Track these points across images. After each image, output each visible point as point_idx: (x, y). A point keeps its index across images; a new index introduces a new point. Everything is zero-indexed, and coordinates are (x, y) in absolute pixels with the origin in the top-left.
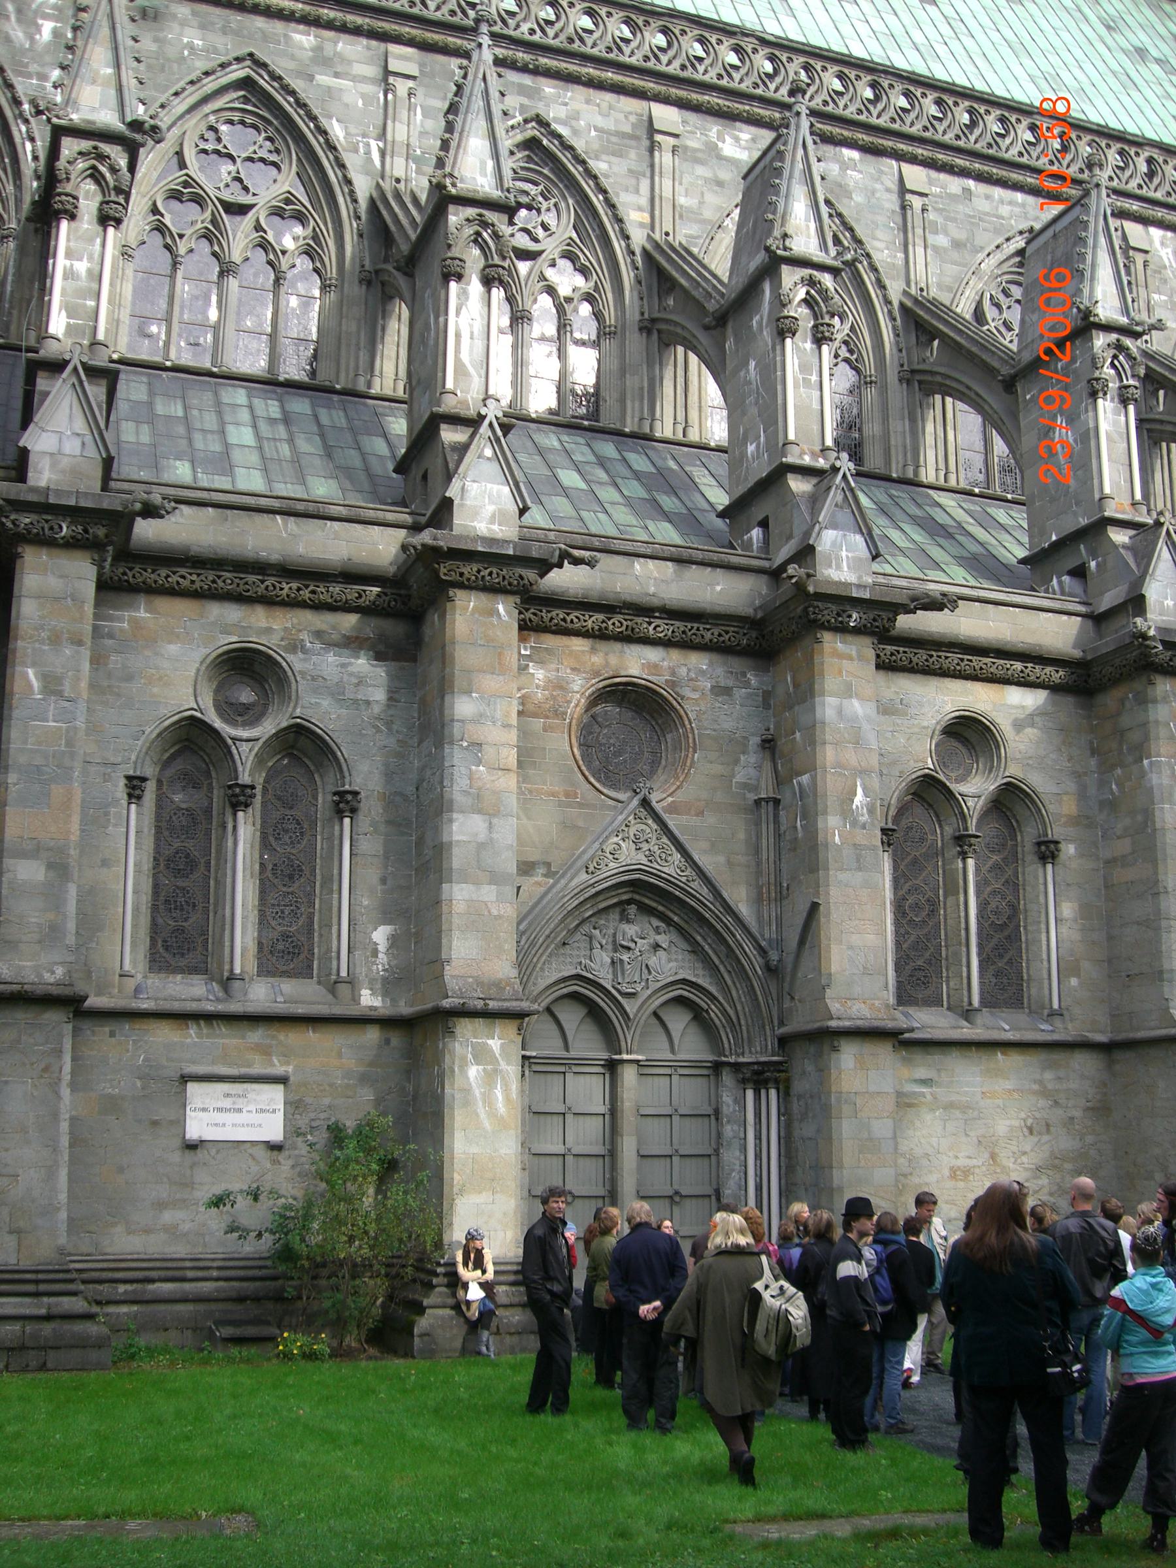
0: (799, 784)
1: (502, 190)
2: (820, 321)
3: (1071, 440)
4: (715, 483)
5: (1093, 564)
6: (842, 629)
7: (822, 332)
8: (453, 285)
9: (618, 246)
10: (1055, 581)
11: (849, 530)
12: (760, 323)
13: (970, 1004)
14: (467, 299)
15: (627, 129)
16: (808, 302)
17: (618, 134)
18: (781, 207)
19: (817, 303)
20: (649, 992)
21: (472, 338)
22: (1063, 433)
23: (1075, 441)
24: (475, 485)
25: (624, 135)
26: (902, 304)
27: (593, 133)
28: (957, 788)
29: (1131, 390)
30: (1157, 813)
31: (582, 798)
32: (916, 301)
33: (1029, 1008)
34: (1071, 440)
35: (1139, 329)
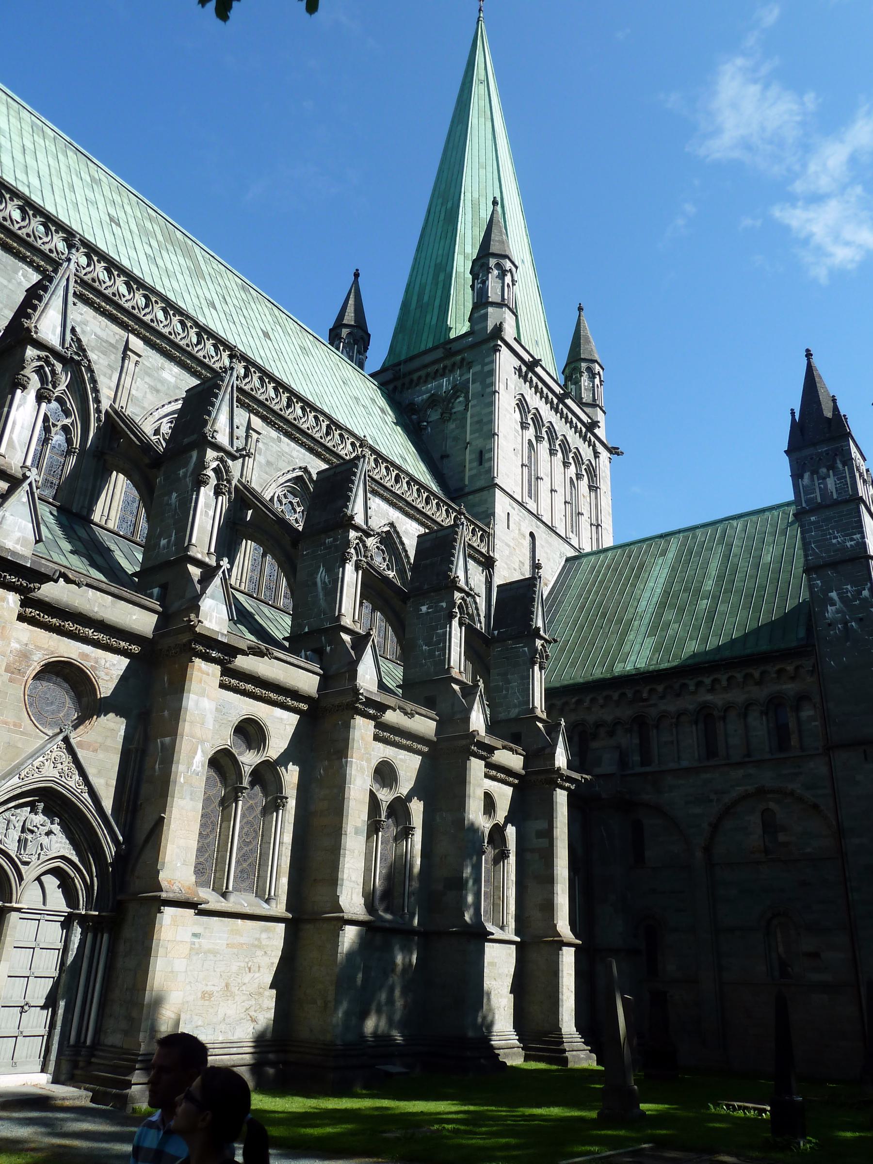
0: (162, 743)
1: (63, 348)
2: (221, 482)
3: (327, 580)
4: (123, 556)
5: (328, 649)
8: (19, 391)
9: (92, 406)
11: (220, 602)
13: (227, 888)
14: (25, 403)
15: (113, 341)
16: (216, 470)
17: (107, 342)
18: (213, 415)
19: (221, 472)
20: (40, 862)
21: (22, 427)
22: (322, 575)
23: (329, 582)
24: (12, 517)
25: (111, 344)
26: (236, 485)
27: (93, 336)
28: (241, 759)
29: (362, 563)
31: (24, 729)
32: (245, 487)
33: (256, 893)
34: (327, 580)
35: (372, 533)
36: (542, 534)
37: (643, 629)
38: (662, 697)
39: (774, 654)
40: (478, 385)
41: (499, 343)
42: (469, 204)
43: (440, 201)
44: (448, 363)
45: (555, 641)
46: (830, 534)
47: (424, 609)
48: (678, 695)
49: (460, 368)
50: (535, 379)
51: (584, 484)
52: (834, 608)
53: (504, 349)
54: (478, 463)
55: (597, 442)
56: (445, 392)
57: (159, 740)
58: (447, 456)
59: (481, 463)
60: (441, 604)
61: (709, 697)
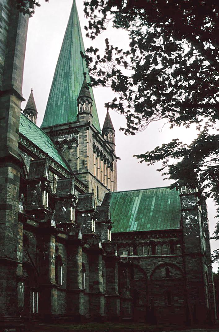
36: (100, 186)
47: (83, 215)
51: (109, 169)
53: (90, 129)
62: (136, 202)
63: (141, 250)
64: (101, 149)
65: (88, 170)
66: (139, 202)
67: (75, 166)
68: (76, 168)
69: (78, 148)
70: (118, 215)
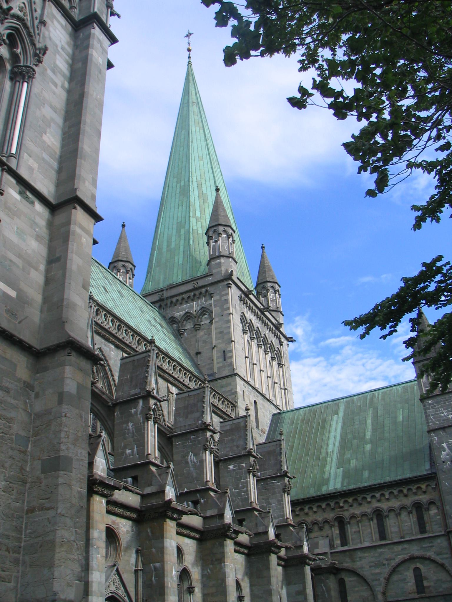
0: (154, 567)
5: (202, 501)
6: (172, 519)
7: (157, 420)
10: (185, 503)
12: (136, 413)
22: (191, 457)
23: (197, 461)
30: (227, 580)
35: (216, 431)
36: (260, 401)
37: (334, 463)
38: (351, 506)
39: (414, 479)
40: (218, 308)
41: (230, 282)
42: (195, 184)
43: (175, 180)
44: (197, 293)
45: (294, 477)
46: (440, 411)
47: (231, 467)
48: (360, 504)
49: (204, 296)
50: (249, 302)
51: (275, 363)
52: (445, 453)
53: (233, 286)
54: (223, 359)
55: (281, 336)
56: (195, 311)
57: (152, 565)
58: (200, 353)
59: (225, 360)
60: (243, 464)
61: (379, 505)
62: (333, 427)
63: (355, 532)
64: (257, 323)
65: (234, 369)
66: (340, 425)
67: (209, 364)
68: (212, 368)
69: (213, 327)
70: (300, 459)
